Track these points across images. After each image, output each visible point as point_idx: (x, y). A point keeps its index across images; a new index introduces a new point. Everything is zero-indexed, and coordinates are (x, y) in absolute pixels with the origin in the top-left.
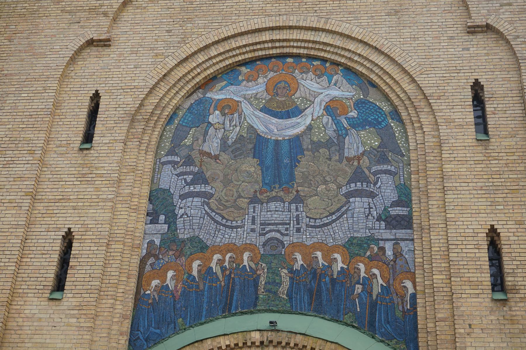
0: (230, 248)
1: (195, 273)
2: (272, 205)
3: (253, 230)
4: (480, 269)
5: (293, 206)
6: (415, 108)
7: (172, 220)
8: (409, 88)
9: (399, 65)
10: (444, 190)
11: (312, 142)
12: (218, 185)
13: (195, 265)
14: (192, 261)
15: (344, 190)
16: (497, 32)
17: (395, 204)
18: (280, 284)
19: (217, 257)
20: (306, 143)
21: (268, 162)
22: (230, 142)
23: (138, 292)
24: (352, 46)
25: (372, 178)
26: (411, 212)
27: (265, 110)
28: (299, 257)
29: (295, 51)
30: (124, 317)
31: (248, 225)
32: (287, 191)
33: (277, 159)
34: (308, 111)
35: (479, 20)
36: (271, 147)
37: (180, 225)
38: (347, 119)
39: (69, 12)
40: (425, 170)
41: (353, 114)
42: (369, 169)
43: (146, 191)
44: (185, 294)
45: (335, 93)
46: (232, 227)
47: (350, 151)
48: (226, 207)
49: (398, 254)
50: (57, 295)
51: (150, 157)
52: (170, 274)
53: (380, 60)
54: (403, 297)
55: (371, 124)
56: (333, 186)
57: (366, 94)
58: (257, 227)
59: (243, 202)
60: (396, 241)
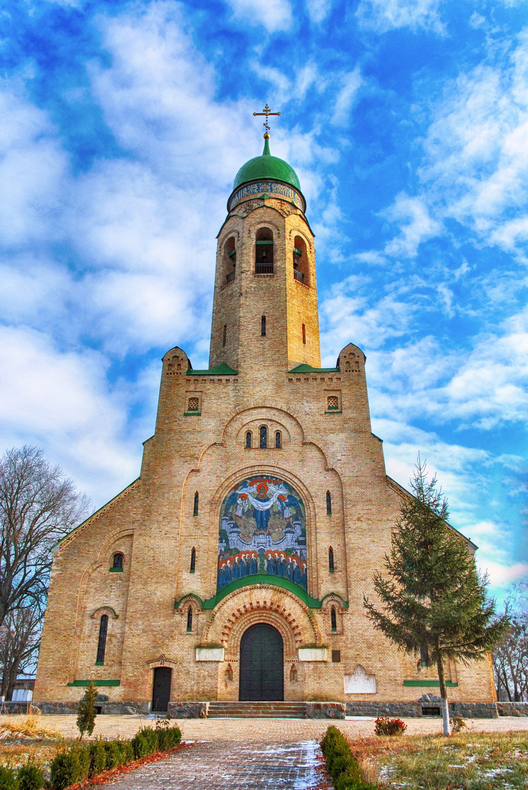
0: (247, 552)
1: (236, 561)
2: (261, 536)
3: (255, 546)
4: (326, 561)
5: (268, 537)
6: (308, 500)
7: (227, 541)
8: (306, 492)
9: (303, 483)
10: (316, 533)
11: (273, 512)
12: (242, 528)
13: (237, 558)
14: (235, 557)
15: (284, 531)
16: (336, 471)
17: (301, 536)
18: (264, 565)
19: (243, 555)
20: (271, 513)
21: (259, 520)
22: (245, 511)
23: (218, 568)
24: (287, 474)
25: (293, 526)
26: (306, 539)
27: (257, 498)
28: (270, 555)
29: (266, 474)
30: (215, 578)
31: (253, 544)
32: (265, 531)
33: (262, 519)
34: (272, 499)
35: (330, 466)
36: (259, 513)
37: (230, 544)
38: (285, 503)
39: (183, 457)
40: (310, 525)
41: (287, 501)
42: (292, 523)
43: (218, 531)
44: (234, 569)
45: (281, 492)
46: (248, 544)
47: (286, 516)
48: (245, 537)
49: (301, 554)
50: (192, 571)
51: (218, 518)
52: (228, 561)
53: (296, 480)
54: (303, 569)
55: (293, 505)
56: (281, 529)
57: (291, 492)
58: (256, 544)
59: (251, 535)
60: (301, 550)
